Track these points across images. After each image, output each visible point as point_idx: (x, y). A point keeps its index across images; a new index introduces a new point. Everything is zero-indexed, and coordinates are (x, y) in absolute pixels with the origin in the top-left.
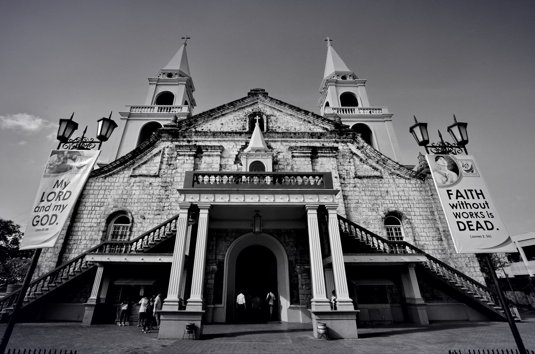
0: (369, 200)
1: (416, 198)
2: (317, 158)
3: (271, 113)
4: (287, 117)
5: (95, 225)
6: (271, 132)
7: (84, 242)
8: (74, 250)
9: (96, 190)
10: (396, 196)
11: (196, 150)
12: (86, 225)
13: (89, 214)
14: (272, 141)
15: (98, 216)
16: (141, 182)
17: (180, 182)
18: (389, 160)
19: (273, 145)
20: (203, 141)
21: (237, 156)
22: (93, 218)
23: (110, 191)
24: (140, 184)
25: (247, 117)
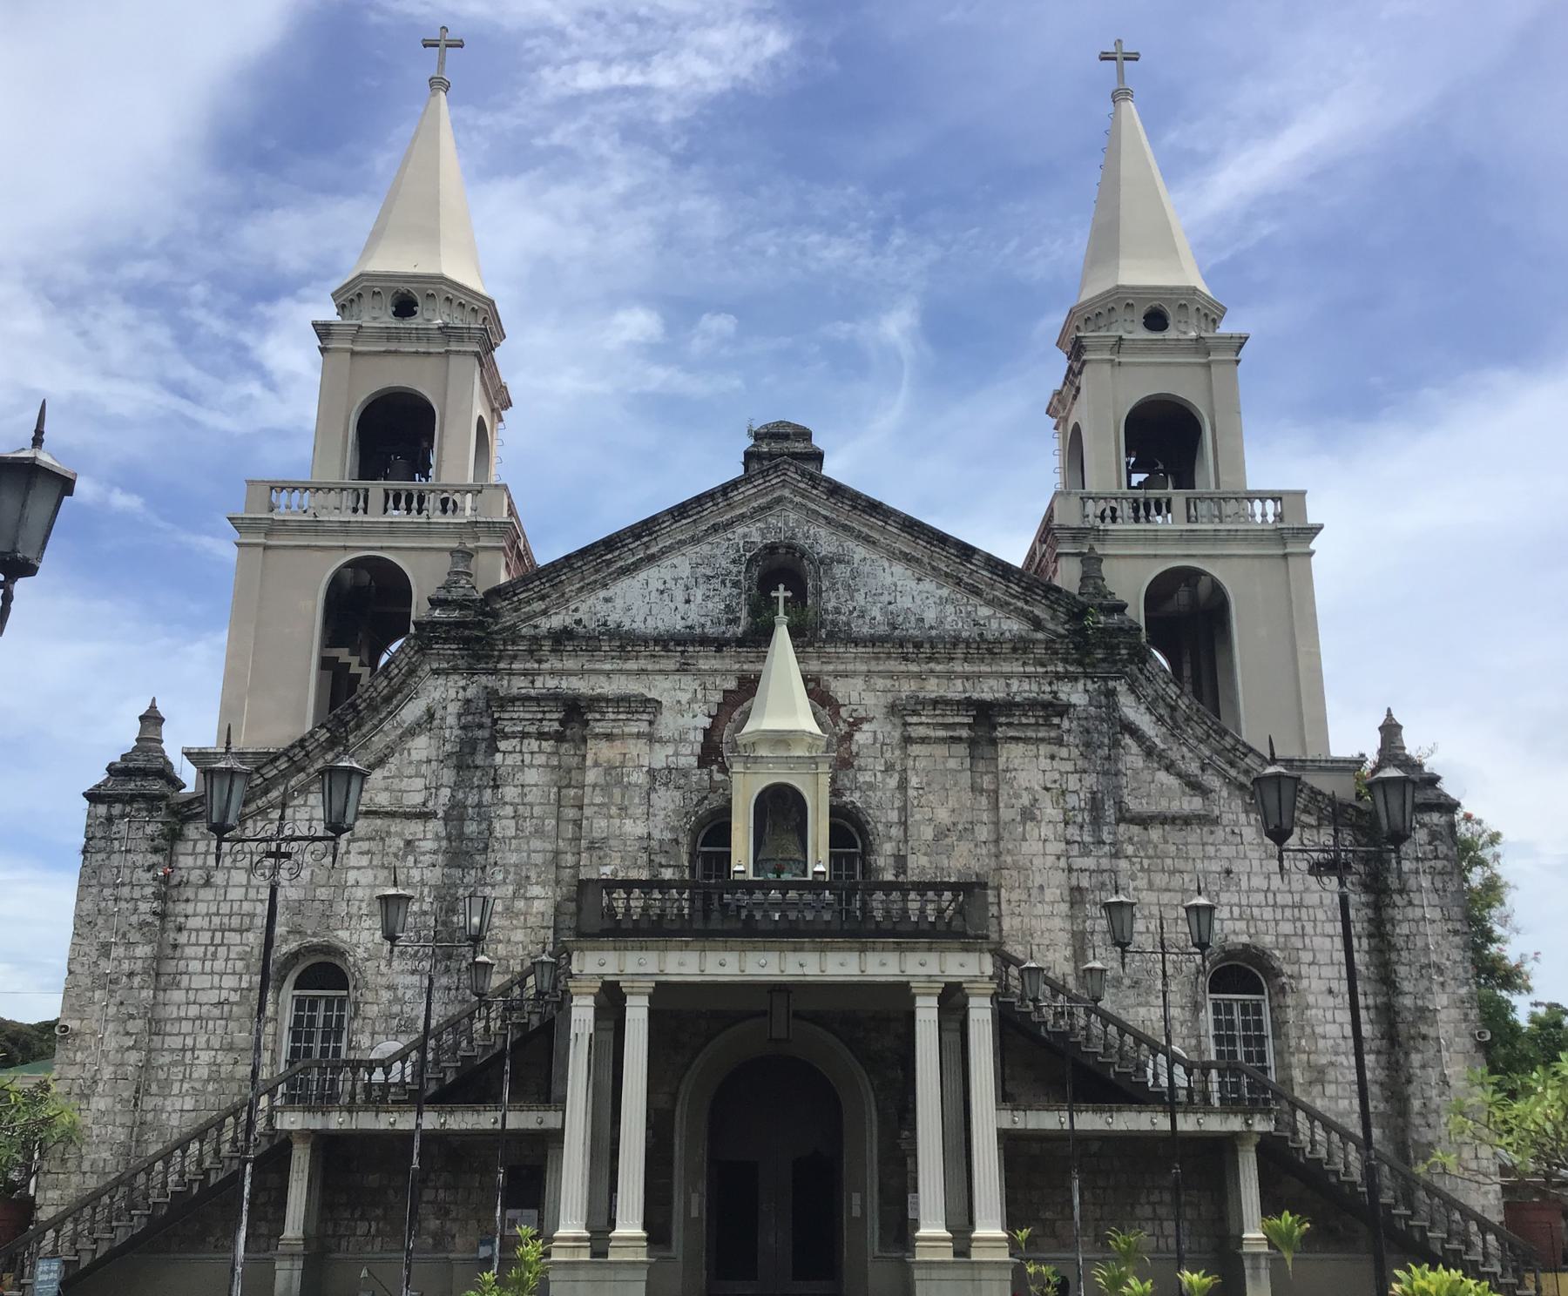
0: (1159, 904)
2: (993, 742)
3: (833, 549)
4: (893, 569)
5: (234, 997)
6: (832, 638)
7: (205, 1057)
8: (176, 1087)
10: (1258, 890)
11: (560, 716)
12: (202, 997)
14: (837, 675)
15: (240, 965)
16: (373, 839)
17: (514, 838)
19: (840, 689)
20: (582, 673)
21: (707, 733)
22: (221, 975)
24: (372, 845)
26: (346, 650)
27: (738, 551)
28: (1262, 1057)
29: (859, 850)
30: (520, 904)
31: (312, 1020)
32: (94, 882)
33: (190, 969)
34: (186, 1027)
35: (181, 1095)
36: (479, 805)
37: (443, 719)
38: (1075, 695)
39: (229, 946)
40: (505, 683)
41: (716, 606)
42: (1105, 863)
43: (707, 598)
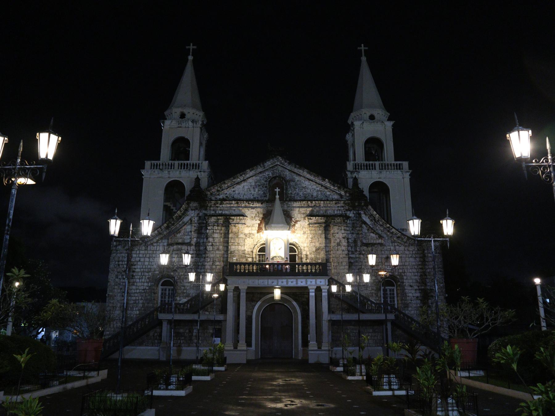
1: (410, 264)
4: (306, 183)
5: (147, 288)
8: (135, 308)
9: (141, 257)
12: (140, 288)
13: (140, 279)
18: (393, 229)
22: (144, 282)
23: (153, 258)
25: (268, 183)
26: (169, 203)
27: (266, 178)
28: (394, 301)
29: (297, 253)
30: (214, 267)
31: (165, 293)
32: (113, 260)
33: (137, 281)
34: (136, 295)
35: (136, 310)
36: (203, 242)
37: (194, 221)
38: (351, 214)
39: (145, 276)
40: (209, 212)
41: (261, 192)
42: (357, 256)
43: (259, 191)
